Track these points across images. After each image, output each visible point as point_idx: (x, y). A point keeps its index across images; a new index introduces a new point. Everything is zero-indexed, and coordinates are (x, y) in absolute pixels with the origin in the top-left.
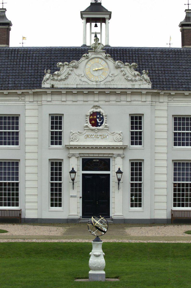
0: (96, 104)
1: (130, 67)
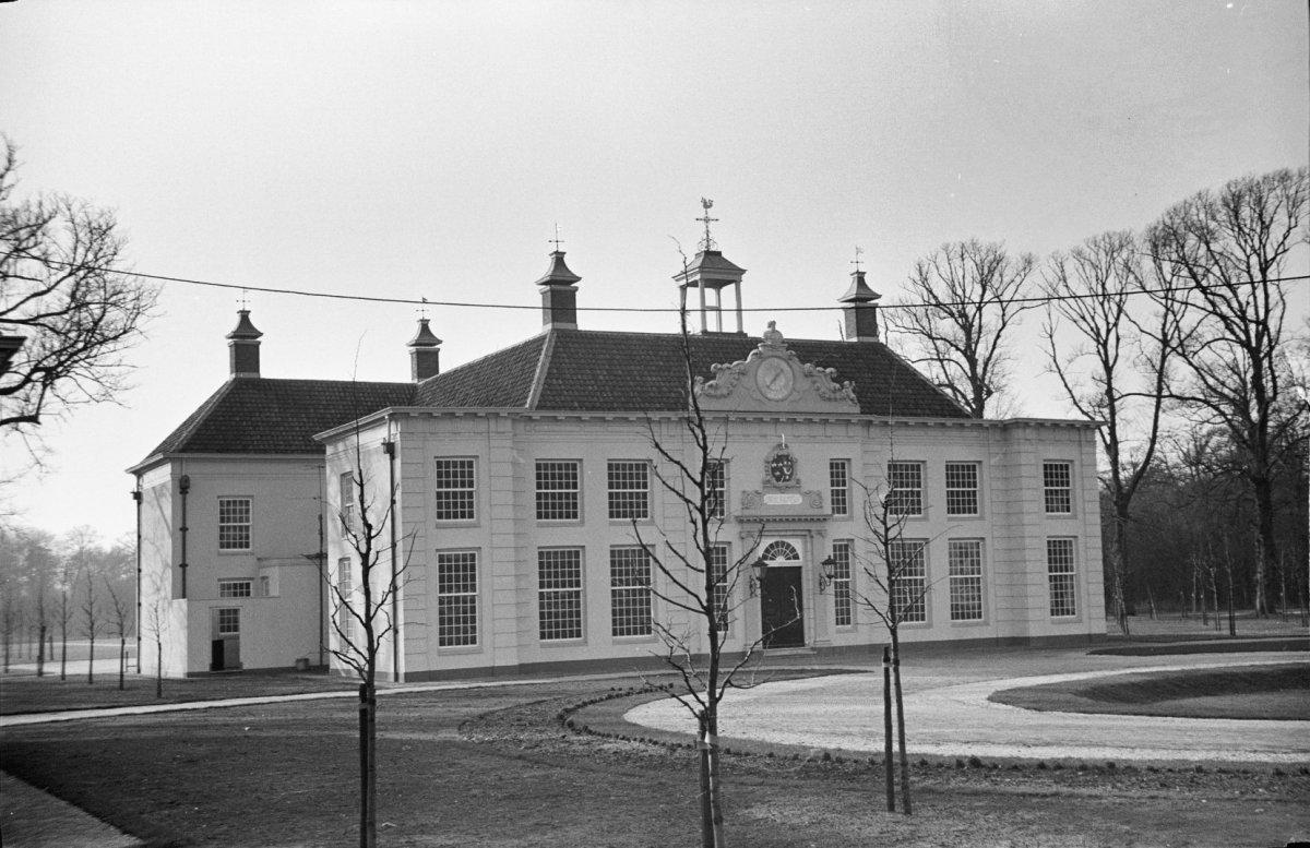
1: (825, 376)
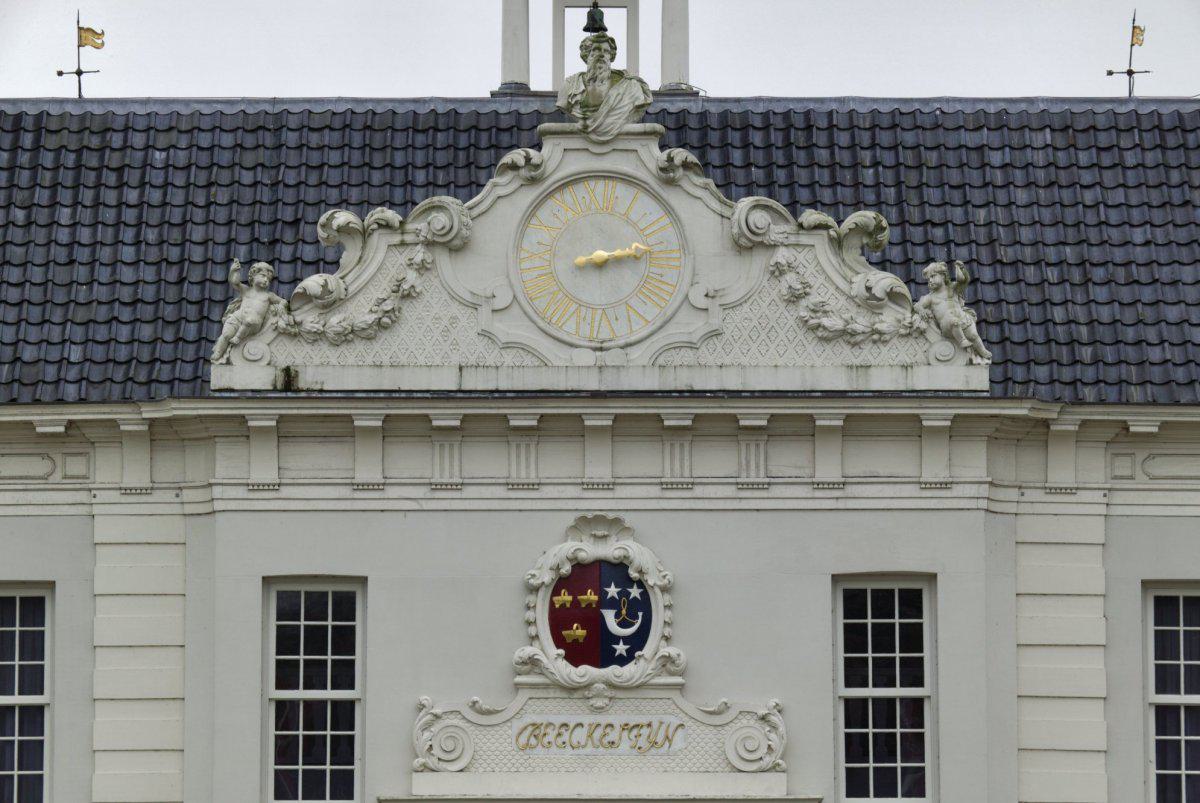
0: (598, 503)
1: (838, 243)
